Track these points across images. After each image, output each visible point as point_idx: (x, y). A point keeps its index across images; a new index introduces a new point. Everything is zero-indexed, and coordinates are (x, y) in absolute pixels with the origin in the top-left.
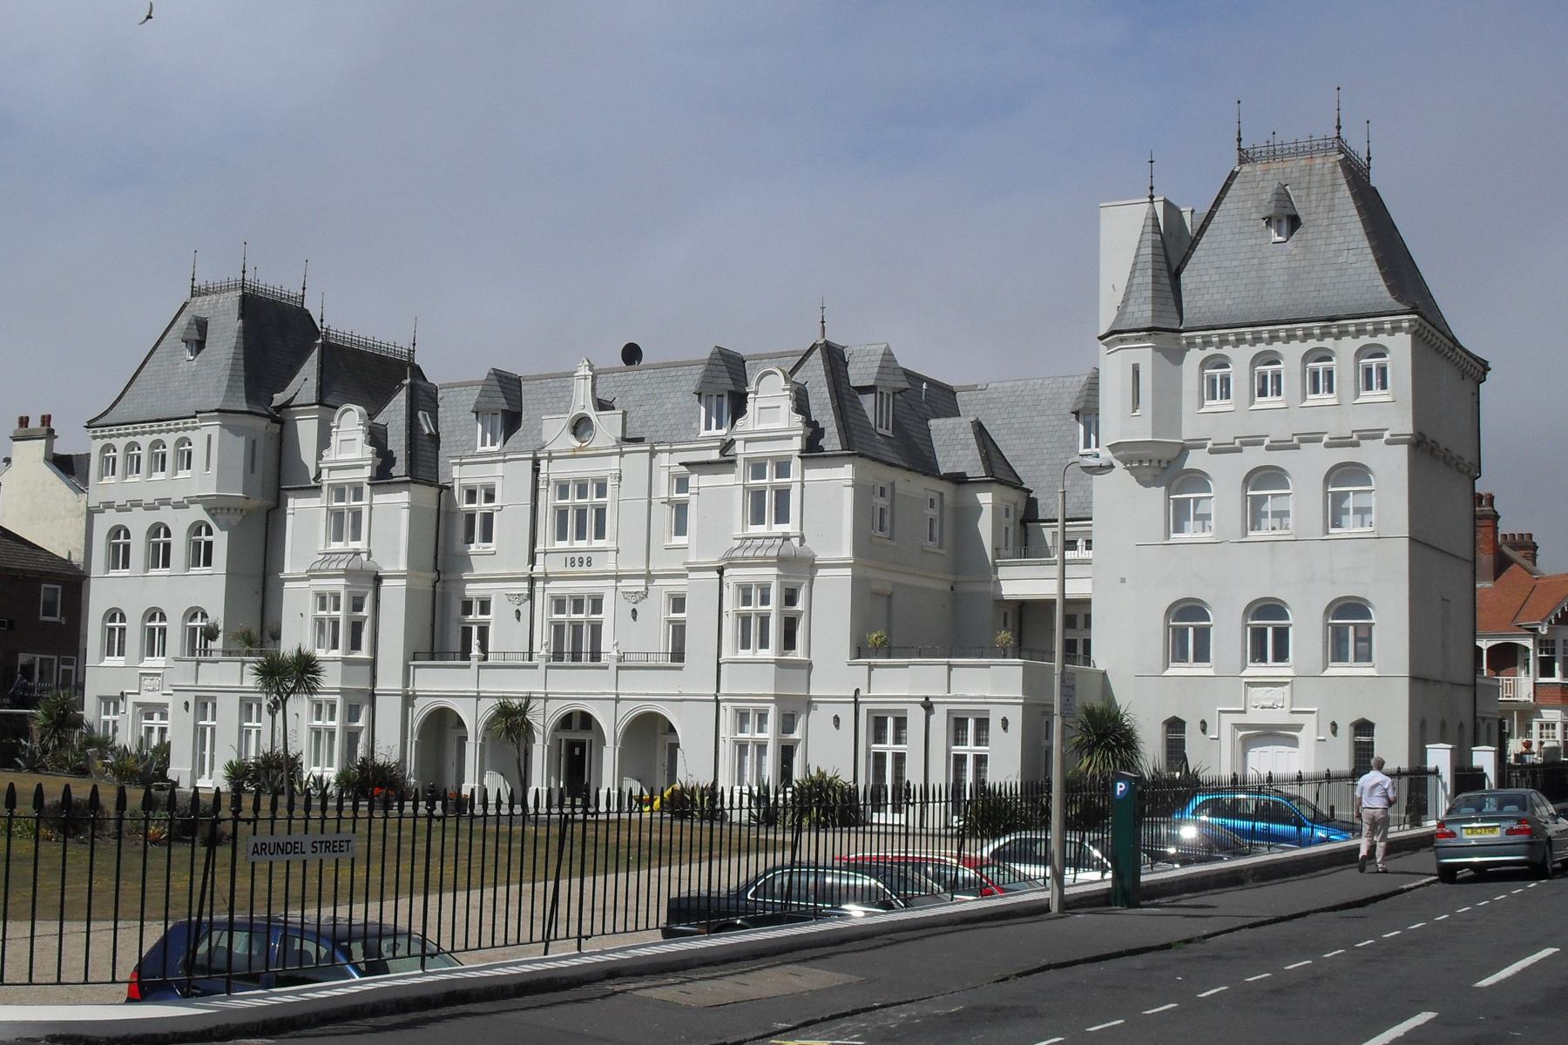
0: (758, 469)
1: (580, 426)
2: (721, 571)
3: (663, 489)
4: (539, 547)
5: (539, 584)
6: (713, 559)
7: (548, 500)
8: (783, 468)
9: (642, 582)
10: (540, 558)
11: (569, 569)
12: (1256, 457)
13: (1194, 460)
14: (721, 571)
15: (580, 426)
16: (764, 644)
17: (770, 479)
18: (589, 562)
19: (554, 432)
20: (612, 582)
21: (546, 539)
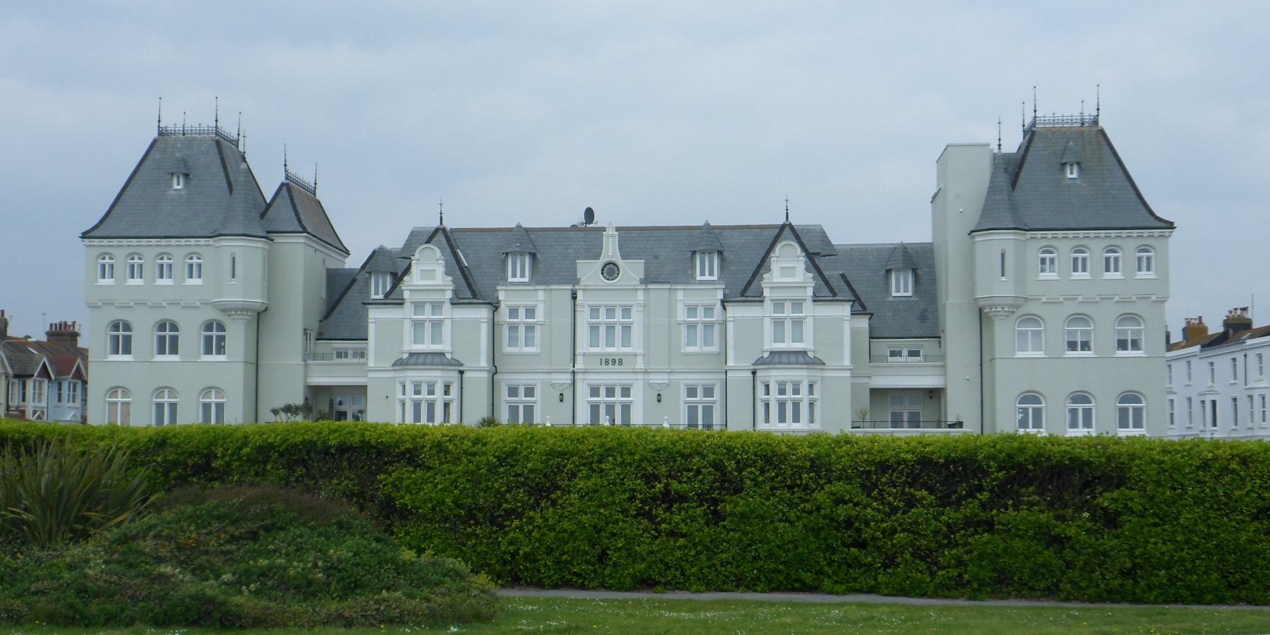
0: (779, 305)
1: (610, 270)
2: (754, 373)
3: (681, 315)
4: (578, 351)
5: (578, 377)
6: (748, 364)
7: (584, 318)
8: (797, 305)
9: (666, 376)
10: (579, 360)
11: (604, 366)
12: (1073, 308)
13: (1032, 308)
14: (754, 373)
15: (610, 270)
16: (796, 419)
17: (788, 312)
18: (621, 362)
19: (589, 271)
20: (640, 376)
21: (583, 346)
